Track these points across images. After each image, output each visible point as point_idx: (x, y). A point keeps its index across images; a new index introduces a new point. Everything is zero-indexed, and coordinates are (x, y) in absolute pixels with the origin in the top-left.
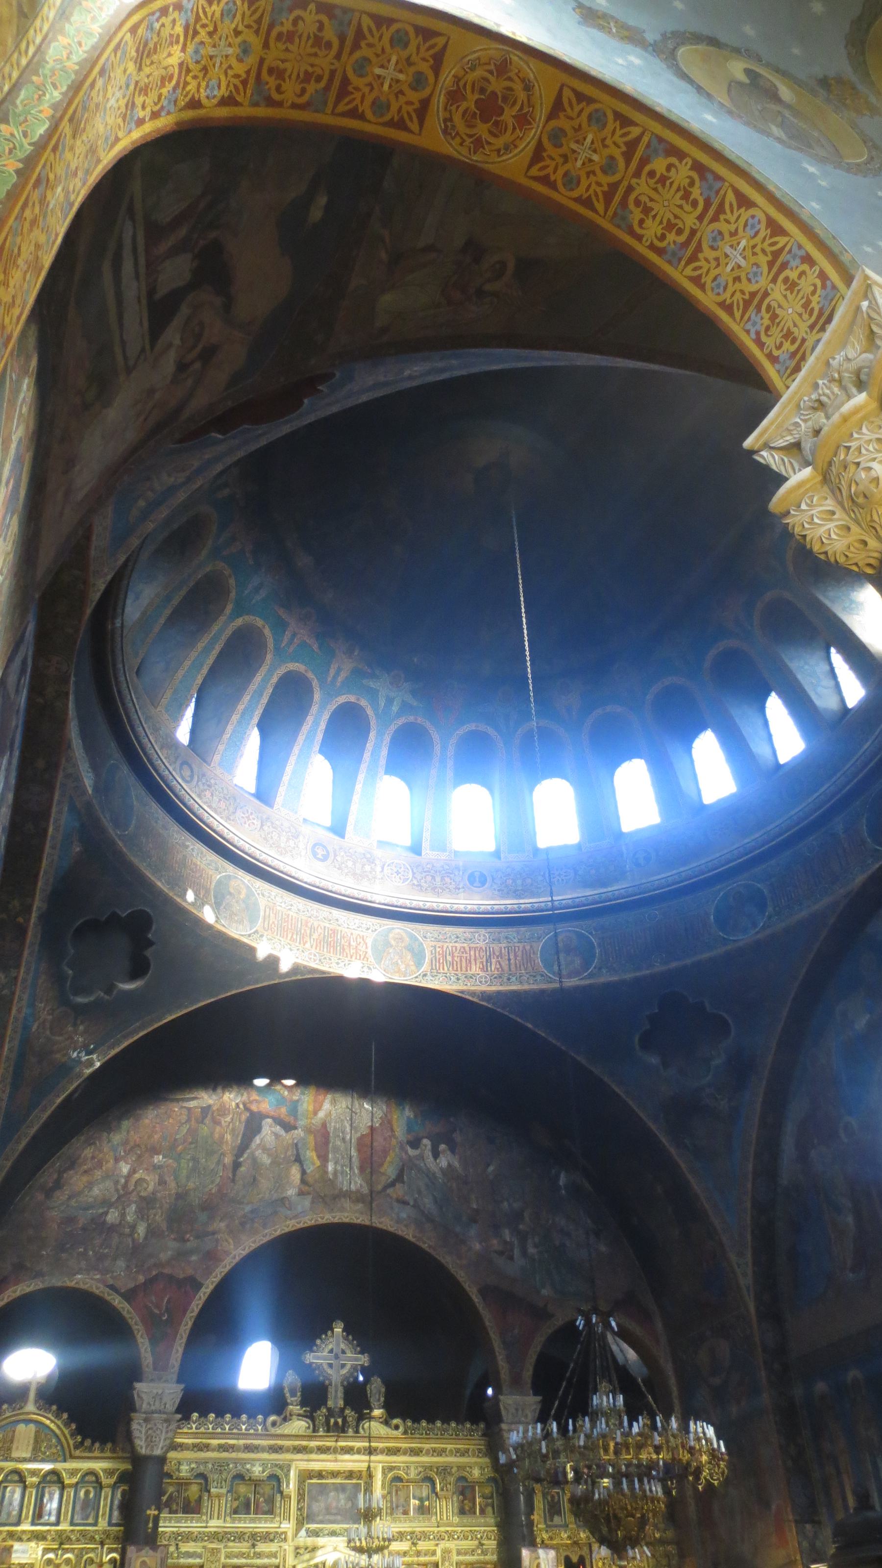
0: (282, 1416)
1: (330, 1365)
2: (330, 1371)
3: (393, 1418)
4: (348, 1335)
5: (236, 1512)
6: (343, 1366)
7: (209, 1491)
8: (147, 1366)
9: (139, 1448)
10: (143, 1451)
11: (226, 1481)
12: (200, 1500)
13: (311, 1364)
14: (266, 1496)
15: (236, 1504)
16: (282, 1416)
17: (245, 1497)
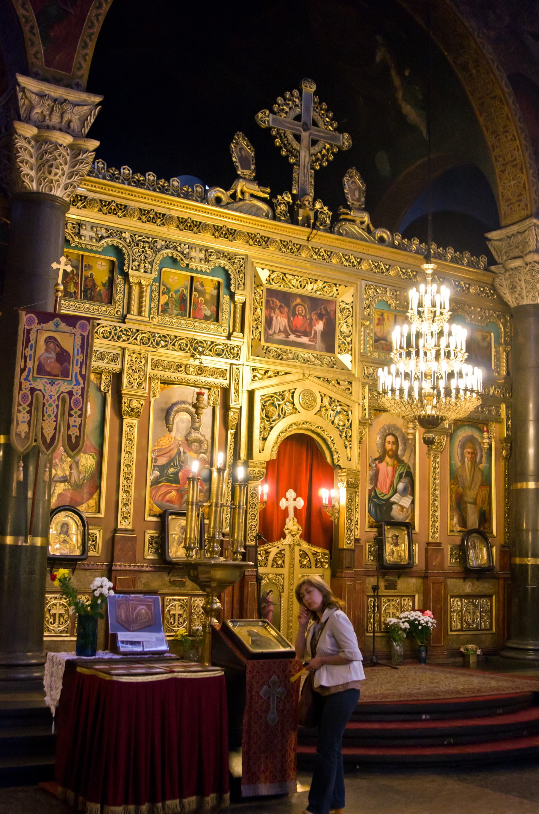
0: (231, 192)
1: (298, 138)
2: (295, 144)
3: (376, 227)
4: (320, 103)
5: (164, 310)
6: (314, 143)
7: (126, 276)
8: (35, 55)
9: (27, 180)
10: (34, 186)
11: (151, 263)
12: (111, 284)
13: (269, 129)
14: (208, 297)
15: (164, 299)
16: (231, 192)
17: (177, 292)
